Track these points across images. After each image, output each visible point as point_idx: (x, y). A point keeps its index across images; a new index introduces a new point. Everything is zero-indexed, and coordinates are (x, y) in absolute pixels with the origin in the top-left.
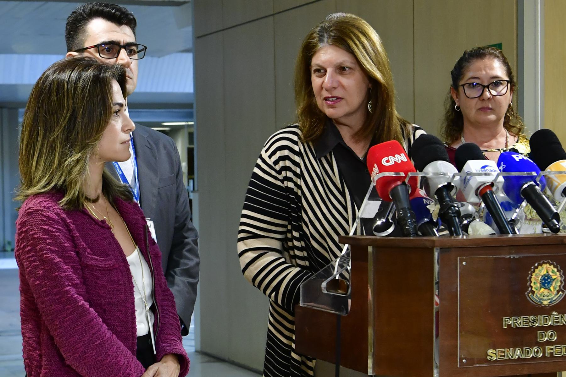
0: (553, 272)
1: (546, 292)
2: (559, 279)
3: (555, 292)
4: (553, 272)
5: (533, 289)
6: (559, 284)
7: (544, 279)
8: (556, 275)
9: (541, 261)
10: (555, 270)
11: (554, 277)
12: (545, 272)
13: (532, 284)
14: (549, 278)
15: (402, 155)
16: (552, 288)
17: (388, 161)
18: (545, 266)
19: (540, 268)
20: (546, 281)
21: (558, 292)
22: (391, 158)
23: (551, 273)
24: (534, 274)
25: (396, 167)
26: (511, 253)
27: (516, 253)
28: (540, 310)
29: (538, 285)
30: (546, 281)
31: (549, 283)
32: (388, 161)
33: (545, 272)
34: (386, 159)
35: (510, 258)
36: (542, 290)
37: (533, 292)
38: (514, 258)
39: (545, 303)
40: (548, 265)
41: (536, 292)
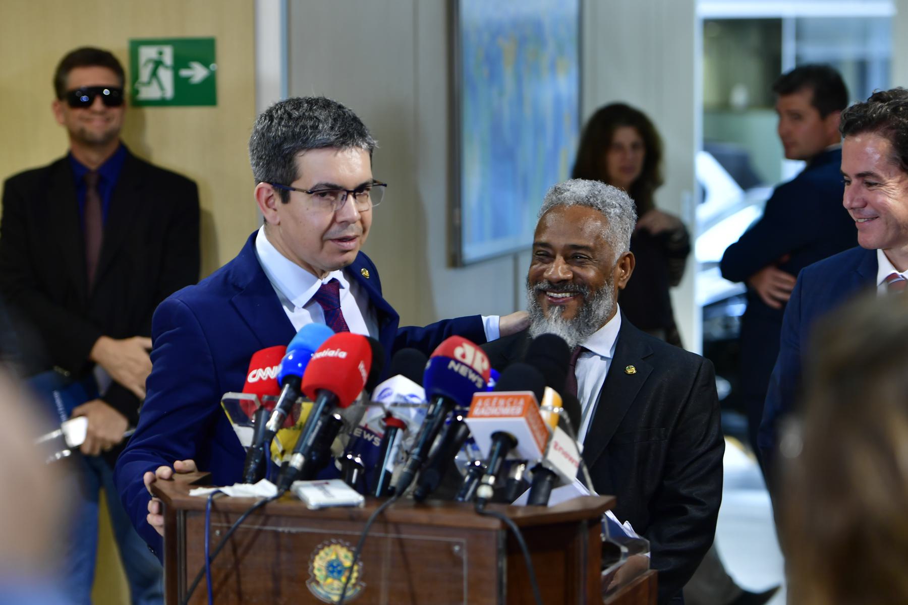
4: (346, 557)
5: (318, 579)
13: (316, 572)
17: (254, 376)
18: (333, 547)
19: (327, 549)
20: (334, 569)
22: (261, 370)
24: (317, 558)
27: (293, 525)
29: (324, 573)
32: (254, 376)
33: (333, 557)
36: (329, 580)
37: (318, 583)
40: (338, 548)
41: (321, 582)
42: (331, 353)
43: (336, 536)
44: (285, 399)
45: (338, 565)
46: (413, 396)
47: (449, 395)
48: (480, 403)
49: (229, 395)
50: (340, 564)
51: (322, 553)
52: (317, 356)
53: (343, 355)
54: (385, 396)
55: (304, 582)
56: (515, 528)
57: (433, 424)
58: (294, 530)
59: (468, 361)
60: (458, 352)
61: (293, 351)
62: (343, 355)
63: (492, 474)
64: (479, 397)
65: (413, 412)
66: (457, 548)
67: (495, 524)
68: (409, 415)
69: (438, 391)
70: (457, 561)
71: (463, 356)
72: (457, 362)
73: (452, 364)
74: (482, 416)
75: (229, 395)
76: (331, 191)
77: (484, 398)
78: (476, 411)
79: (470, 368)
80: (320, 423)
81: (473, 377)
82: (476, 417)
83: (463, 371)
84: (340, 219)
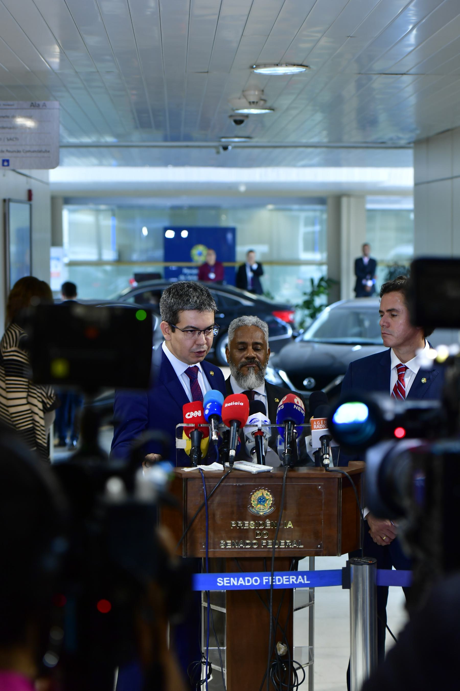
0: (267, 494)
1: (262, 507)
2: (272, 499)
3: (268, 507)
4: (267, 494)
5: (253, 505)
6: (271, 502)
7: (260, 499)
8: (269, 497)
9: (257, 488)
10: (269, 493)
11: (267, 498)
12: (261, 495)
13: (252, 502)
14: (263, 498)
15: (200, 411)
16: (266, 505)
17: (189, 415)
18: (261, 490)
19: (257, 492)
20: (262, 500)
21: (271, 507)
23: (265, 496)
24: (253, 496)
25: (193, 420)
26: (237, 482)
28: (256, 518)
29: (256, 502)
30: (262, 500)
31: (264, 502)
32: (189, 415)
33: (261, 495)
34: (188, 413)
35: (236, 485)
36: (259, 506)
37: (253, 507)
38: (239, 485)
39: (261, 514)
40: (263, 490)
41: (255, 507)
42: (236, 404)
43: (262, 486)
44: (214, 426)
45: (263, 498)
46: (266, 421)
47: (294, 420)
48: (315, 423)
49: (179, 425)
50: (264, 498)
51: (255, 494)
52: (226, 405)
53: (242, 404)
54: (255, 422)
55: (246, 507)
56: (350, 477)
57: (290, 433)
58: (241, 484)
59: (300, 404)
60: (296, 401)
61: (211, 404)
62: (242, 404)
63: (327, 454)
64: (314, 421)
65: (268, 429)
66: (320, 487)
67: (340, 475)
68: (266, 430)
69: (290, 418)
70: (319, 493)
71: (298, 402)
72: (297, 405)
73: (295, 406)
74: (318, 429)
75: (179, 425)
76: (194, 330)
77: (316, 421)
78: (315, 427)
79: (301, 407)
80: (237, 435)
81: (302, 412)
82: (315, 429)
83: (299, 409)
84: (197, 343)
